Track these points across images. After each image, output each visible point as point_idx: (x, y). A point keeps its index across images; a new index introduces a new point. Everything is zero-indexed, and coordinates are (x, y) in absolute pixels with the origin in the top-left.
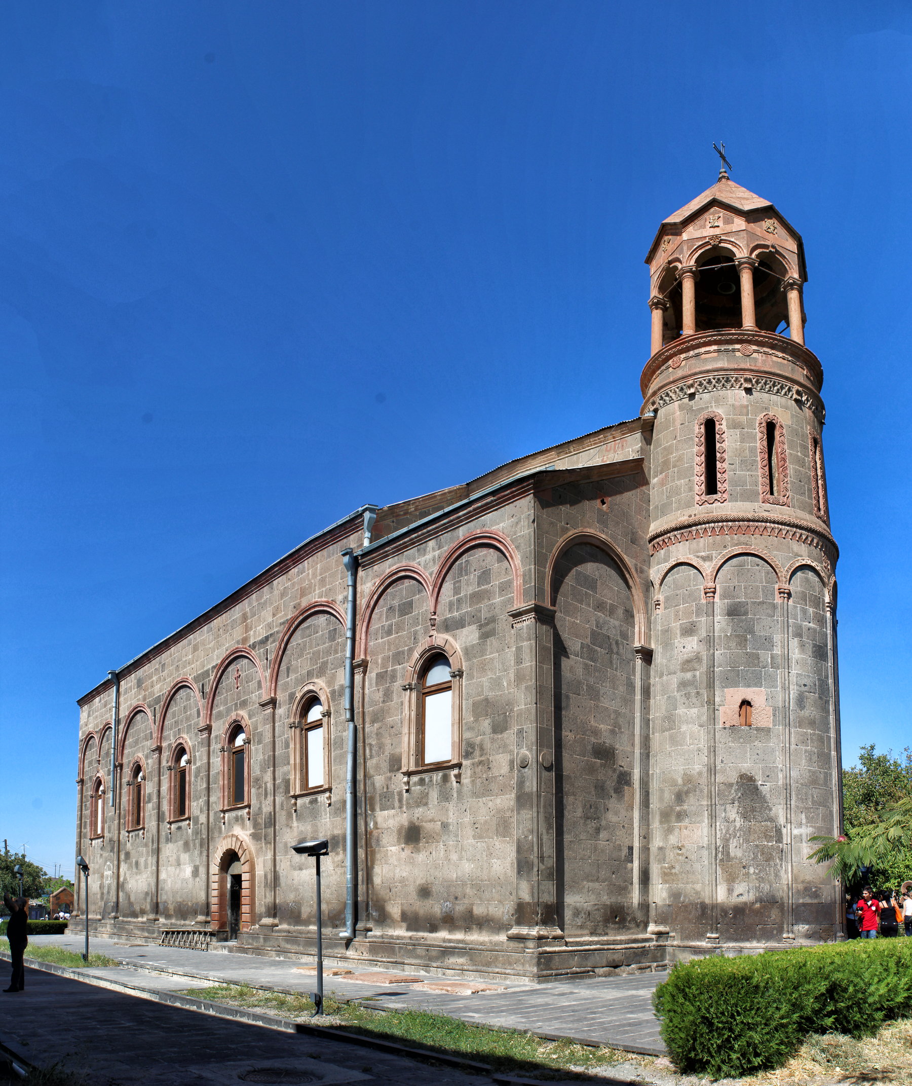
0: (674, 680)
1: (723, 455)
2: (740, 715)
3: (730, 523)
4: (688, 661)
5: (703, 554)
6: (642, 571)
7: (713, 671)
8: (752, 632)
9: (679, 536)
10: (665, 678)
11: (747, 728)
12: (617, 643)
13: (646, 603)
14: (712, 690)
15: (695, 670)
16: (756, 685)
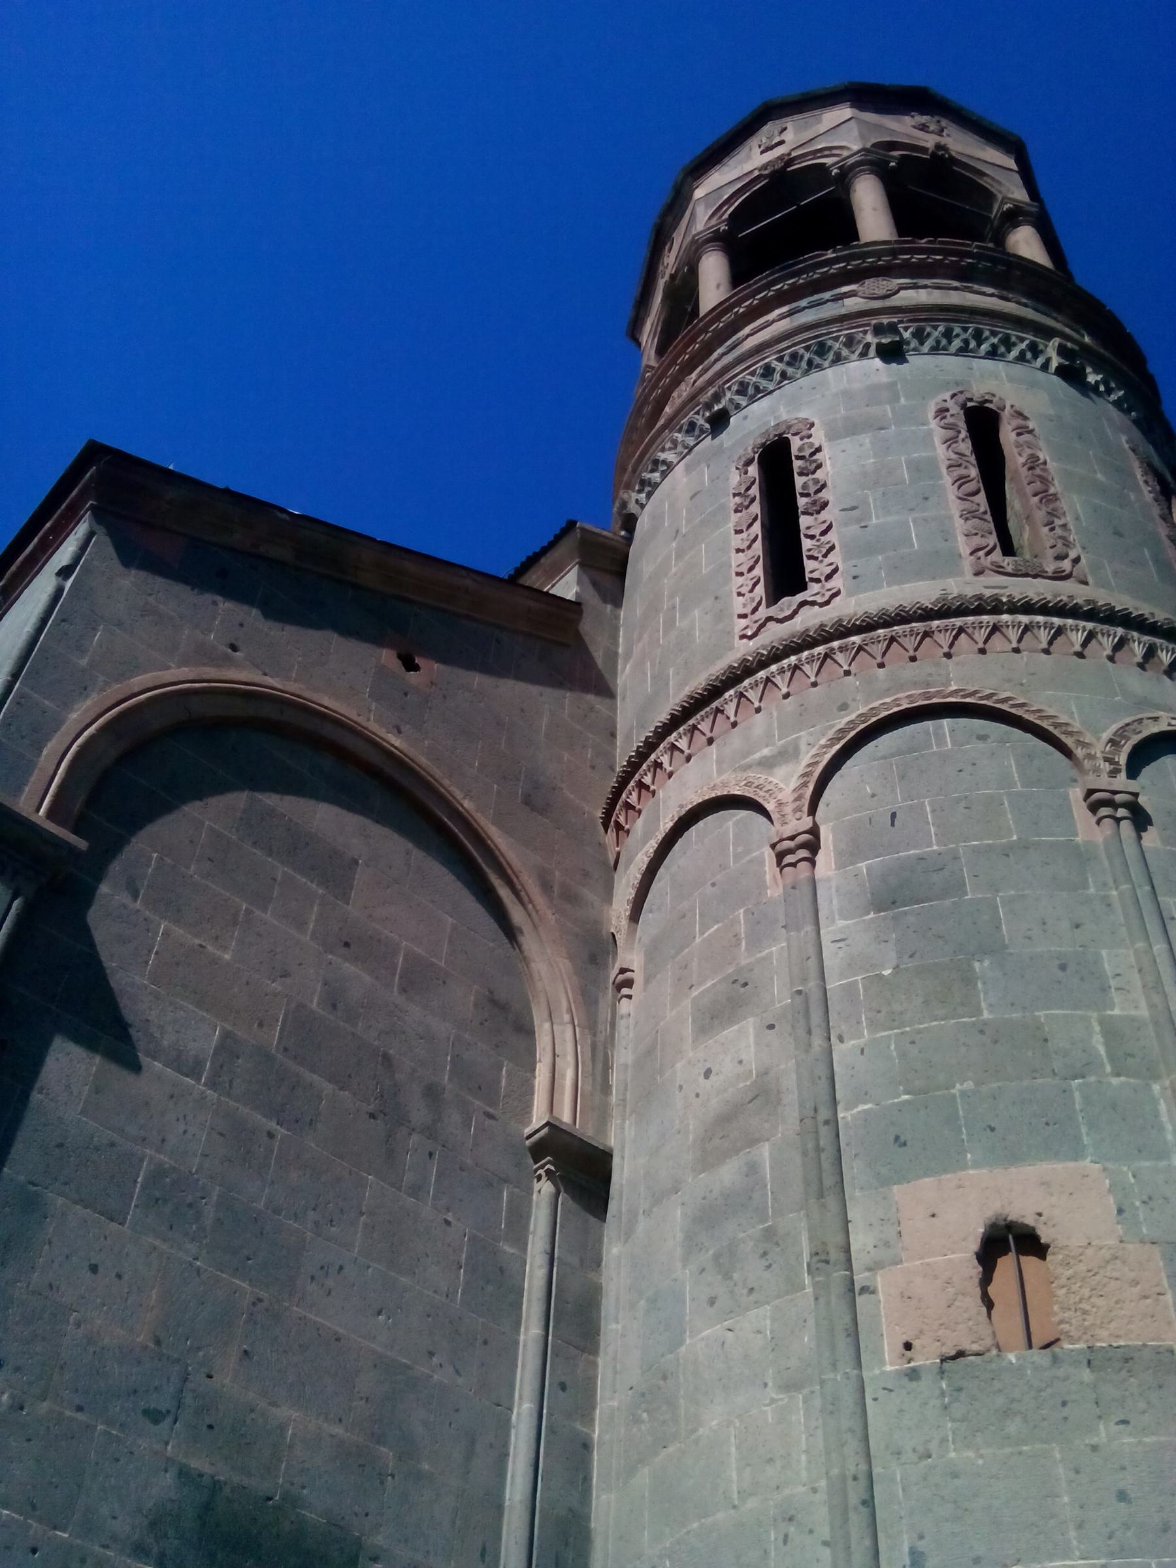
0: (676, 1216)
1: (820, 495)
2: (989, 1304)
3: (856, 639)
4: (727, 1118)
5: (766, 752)
6: (570, 897)
7: (833, 1122)
8: (994, 948)
9: (683, 744)
10: (642, 1225)
11: (1039, 1357)
12: (432, 1093)
13: (588, 998)
14: (832, 1202)
15: (753, 1142)
16: (1050, 1151)
